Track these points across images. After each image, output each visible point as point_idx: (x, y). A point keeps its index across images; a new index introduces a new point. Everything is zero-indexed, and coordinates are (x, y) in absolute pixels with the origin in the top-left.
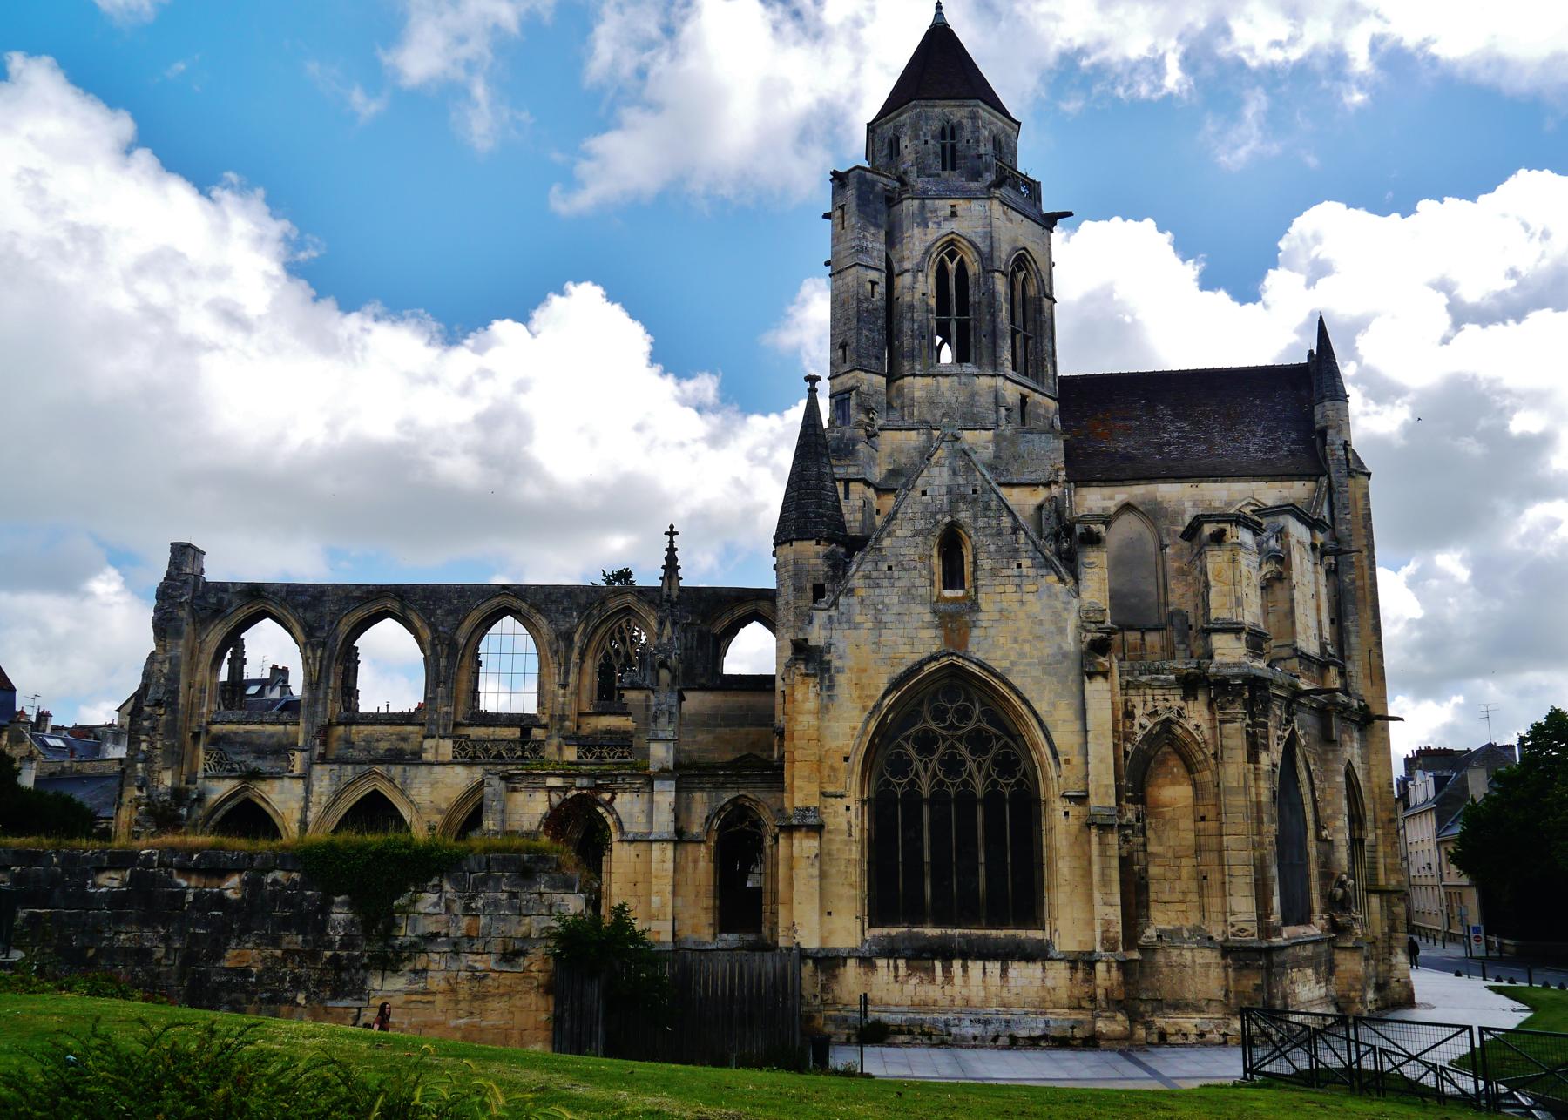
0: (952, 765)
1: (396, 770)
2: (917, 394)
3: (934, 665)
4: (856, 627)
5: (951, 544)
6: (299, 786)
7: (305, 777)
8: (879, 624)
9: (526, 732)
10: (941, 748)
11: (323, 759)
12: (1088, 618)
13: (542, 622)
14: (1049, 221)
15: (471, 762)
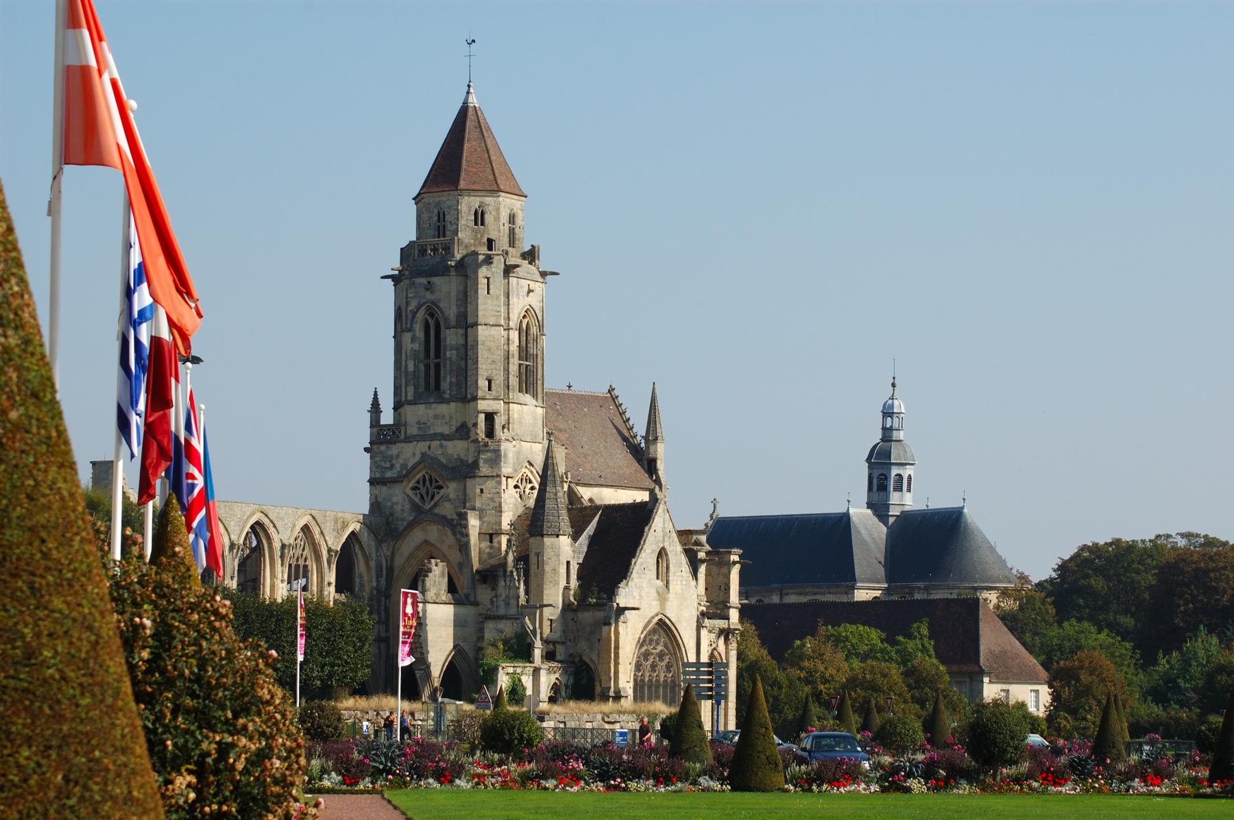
2: (516, 416)
3: (656, 619)
4: (634, 598)
10: (651, 659)
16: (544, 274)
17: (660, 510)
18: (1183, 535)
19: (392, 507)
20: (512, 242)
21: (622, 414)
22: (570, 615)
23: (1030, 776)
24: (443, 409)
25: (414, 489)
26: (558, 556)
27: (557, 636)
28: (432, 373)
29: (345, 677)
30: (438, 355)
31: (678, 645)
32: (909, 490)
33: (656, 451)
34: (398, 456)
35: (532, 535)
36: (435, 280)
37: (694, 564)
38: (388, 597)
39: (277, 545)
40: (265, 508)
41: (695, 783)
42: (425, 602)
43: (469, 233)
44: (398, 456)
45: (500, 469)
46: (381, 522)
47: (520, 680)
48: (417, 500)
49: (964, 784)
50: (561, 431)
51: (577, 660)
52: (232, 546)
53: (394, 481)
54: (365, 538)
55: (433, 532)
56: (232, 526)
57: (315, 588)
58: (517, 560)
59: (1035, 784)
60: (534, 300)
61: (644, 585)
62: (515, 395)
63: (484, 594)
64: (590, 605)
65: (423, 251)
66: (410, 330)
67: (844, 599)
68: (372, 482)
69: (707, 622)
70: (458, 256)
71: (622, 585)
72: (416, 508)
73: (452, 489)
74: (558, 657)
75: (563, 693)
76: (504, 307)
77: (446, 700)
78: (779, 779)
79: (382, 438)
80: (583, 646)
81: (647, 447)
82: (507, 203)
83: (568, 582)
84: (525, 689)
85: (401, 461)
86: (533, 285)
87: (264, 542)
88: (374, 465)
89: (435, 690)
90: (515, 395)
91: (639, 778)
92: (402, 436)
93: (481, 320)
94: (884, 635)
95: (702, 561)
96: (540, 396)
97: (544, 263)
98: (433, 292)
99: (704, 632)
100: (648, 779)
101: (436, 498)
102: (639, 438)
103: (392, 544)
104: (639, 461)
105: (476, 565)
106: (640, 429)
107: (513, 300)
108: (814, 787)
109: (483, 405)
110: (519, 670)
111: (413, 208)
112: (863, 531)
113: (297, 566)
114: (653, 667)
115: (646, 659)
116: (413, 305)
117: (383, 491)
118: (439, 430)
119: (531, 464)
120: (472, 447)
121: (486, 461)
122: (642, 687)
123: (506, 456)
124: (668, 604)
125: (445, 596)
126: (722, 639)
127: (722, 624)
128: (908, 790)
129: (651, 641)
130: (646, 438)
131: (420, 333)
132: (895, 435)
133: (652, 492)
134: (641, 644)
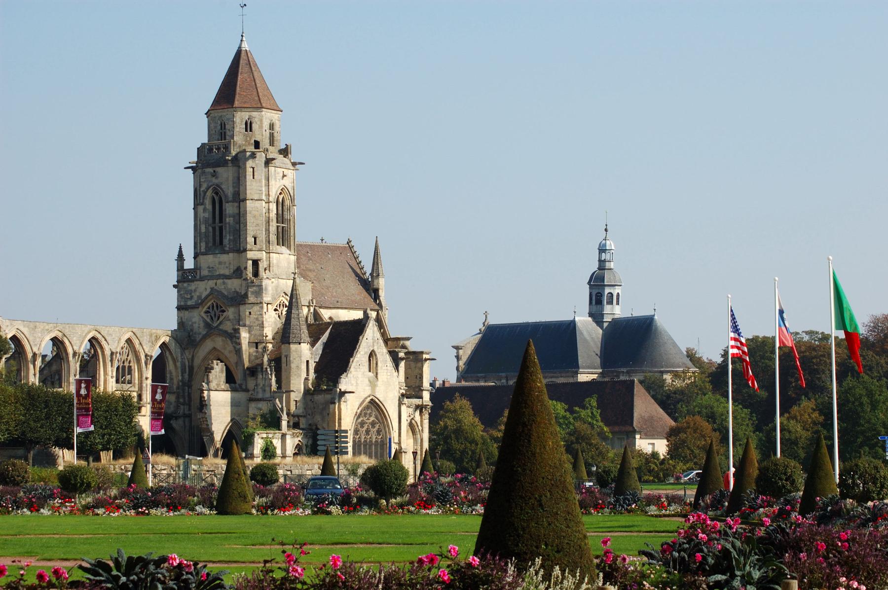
2: (275, 262)
3: (369, 399)
4: (352, 385)
16: (294, 164)
17: (371, 325)
18: (807, 333)
19: (192, 325)
20: (272, 143)
21: (356, 258)
22: (309, 397)
23: (410, 503)
24: (225, 258)
25: (207, 312)
26: (300, 357)
27: (300, 411)
28: (217, 233)
29: (119, 442)
30: (221, 221)
31: (385, 417)
32: (618, 303)
33: (378, 284)
34: (195, 291)
35: (283, 343)
36: (219, 170)
37: (396, 361)
38: (190, 387)
39: (108, 353)
40: (98, 328)
41: (193, 510)
42: (209, 390)
43: (241, 137)
44: (195, 291)
45: (262, 298)
46: (184, 337)
47: (271, 442)
48: (208, 320)
49: (366, 508)
50: (310, 270)
51: (314, 428)
52: (75, 354)
53: (193, 307)
54: (173, 346)
55: (219, 342)
56: (75, 340)
57: (137, 382)
58: (270, 361)
59: (412, 509)
60: (287, 182)
61: (360, 376)
62: (274, 247)
63: (251, 383)
64: (322, 390)
65: (210, 150)
66: (202, 204)
67: (571, 380)
68: (179, 308)
69: (406, 400)
70: (234, 153)
71: (343, 376)
72: (208, 325)
73: (231, 312)
74: (301, 426)
75: (304, 451)
76: (263, 188)
77: (191, 457)
78: (245, 507)
79: (185, 277)
80: (318, 418)
81: (373, 281)
82: (268, 116)
83: (308, 375)
84: (275, 448)
85: (198, 294)
86: (286, 172)
87: (99, 350)
88: (180, 296)
89: (217, 450)
90: (274, 247)
91: (158, 507)
92: (198, 277)
93: (248, 196)
94: (566, 407)
95: (402, 359)
96: (292, 247)
97: (294, 157)
98: (217, 178)
99: (403, 408)
100: (163, 507)
101: (221, 319)
102: (368, 274)
103: (192, 350)
104: (367, 290)
105: (247, 364)
106: (368, 269)
107: (272, 182)
108: (269, 512)
109: (251, 255)
110: (270, 436)
111: (205, 120)
112: (585, 333)
113: (124, 367)
114: (368, 432)
115: (362, 427)
116: (204, 186)
117: (186, 314)
118: (222, 272)
119: (286, 294)
120: (244, 283)
121: (252, 293)
122: (359, 446)
123: (266, 289)
124: (377, 389)
125: (224, 385)
126: (418, 411)
127: (417, 401)
128: (329, 513)
129: (366, 414)
130: (371, 274)
131: (209, 206)
132: (607, 265)
133: (365, 313)
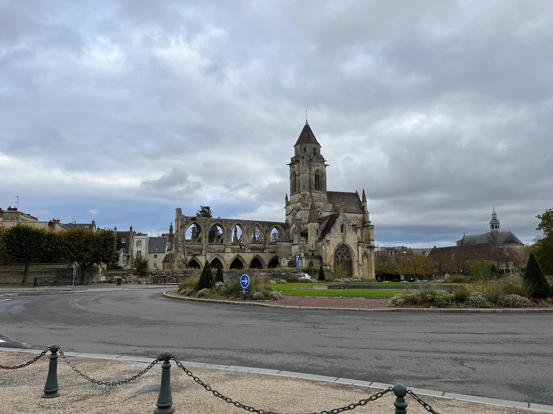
0: (342, 257)
1: (221, 254)
5: (342, 227)
6: (204, 257)
7: (205, 255)
8: (335, 238)
9: (241, 247)
10: (341, 255)
11: (209, 252)
12: (358, 238)
13: (244, 226)
14: (326, 166)
15: (234, 252)
24: (297, 195)
68: (286, 215)
79: (288, 204)
80: (320, 252)
95: (359, 228)
99: (360, 247)
106: (361, 199)
114: (342, 257)
127: (368, 245)
131: (293, 179)
134: (336, 251)
